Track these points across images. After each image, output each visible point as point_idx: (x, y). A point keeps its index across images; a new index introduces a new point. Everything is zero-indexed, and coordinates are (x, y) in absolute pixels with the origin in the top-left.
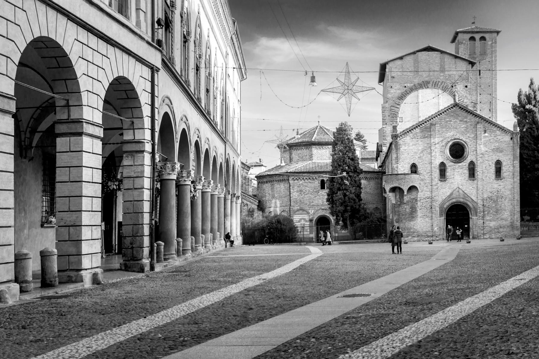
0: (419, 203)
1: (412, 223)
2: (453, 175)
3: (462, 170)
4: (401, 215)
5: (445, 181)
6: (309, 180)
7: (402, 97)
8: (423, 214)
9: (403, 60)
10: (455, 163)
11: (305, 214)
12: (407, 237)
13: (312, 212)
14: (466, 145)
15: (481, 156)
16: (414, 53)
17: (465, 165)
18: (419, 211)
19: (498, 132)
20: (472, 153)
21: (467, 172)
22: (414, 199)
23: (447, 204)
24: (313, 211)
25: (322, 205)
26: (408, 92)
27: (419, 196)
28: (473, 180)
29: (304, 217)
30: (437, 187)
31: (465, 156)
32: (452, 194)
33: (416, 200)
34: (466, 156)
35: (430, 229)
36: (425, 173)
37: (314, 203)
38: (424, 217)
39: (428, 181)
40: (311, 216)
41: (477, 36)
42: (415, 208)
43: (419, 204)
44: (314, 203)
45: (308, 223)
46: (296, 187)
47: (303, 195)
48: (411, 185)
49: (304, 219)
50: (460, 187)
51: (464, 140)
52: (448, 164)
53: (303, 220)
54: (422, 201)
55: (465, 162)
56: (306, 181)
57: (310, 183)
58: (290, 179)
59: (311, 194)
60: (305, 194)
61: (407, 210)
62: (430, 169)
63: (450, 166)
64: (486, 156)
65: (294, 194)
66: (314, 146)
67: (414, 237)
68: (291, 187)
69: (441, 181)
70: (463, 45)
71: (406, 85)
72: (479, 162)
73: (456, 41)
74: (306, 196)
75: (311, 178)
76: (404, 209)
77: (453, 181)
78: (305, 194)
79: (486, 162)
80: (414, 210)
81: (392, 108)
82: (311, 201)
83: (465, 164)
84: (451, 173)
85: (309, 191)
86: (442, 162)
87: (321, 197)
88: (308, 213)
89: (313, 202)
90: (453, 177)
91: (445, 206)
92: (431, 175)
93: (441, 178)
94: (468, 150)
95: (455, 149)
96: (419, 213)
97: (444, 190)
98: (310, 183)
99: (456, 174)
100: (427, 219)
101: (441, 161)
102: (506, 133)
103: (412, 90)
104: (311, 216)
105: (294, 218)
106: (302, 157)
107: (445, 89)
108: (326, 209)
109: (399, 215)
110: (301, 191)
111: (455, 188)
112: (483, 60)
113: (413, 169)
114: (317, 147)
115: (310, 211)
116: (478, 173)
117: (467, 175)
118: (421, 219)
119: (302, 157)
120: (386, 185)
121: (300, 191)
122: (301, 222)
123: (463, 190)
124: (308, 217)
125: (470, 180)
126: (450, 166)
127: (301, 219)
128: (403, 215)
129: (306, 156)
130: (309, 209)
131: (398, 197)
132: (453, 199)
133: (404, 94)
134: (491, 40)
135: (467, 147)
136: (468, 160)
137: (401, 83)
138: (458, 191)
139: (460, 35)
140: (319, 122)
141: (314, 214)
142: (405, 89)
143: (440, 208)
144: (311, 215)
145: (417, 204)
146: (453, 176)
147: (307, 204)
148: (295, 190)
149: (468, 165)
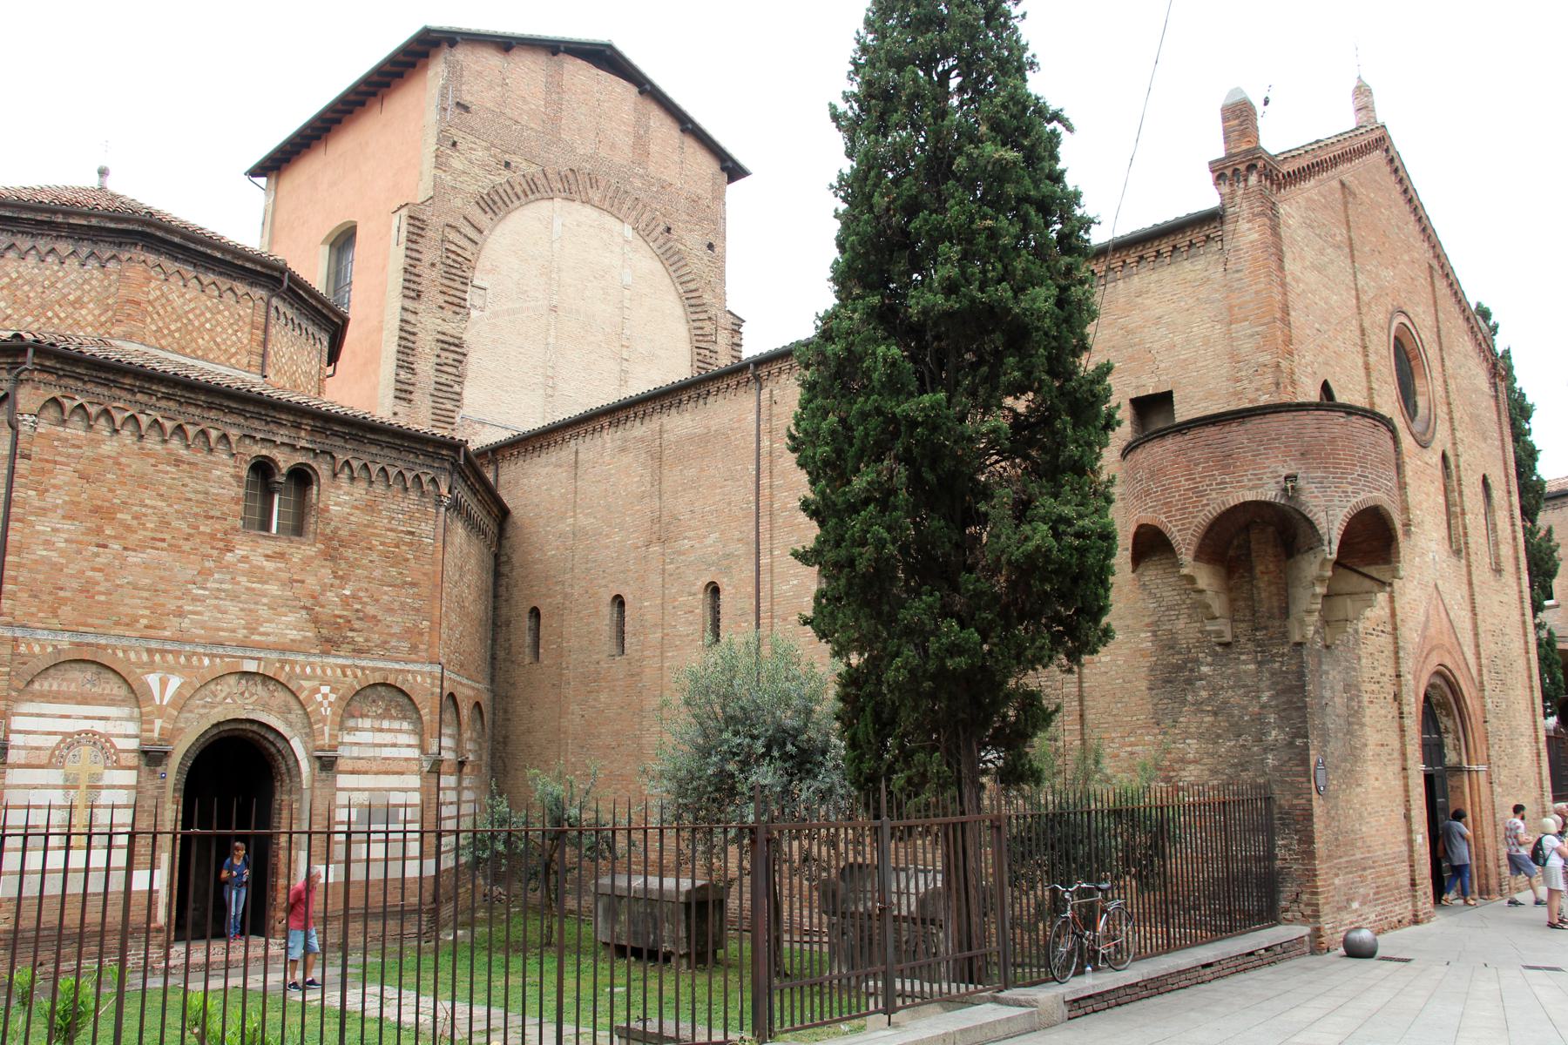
6: (175, 443)
7: (494, 204)
9: (509, 59)
11: (112, 702)
13: (165, 686)
16: (554, 48)
24: (175, 682)
25: (242, 645)
26: (518, 189)
29: (99, 726)
37: (186, 623)
40: (158, 723)
44: (186, 623)
45: (130, 777)
46: (63, 475)
47: (116, 546)
49: (100, 742)
53: (86, 751)
56: (152, 442)
57: (178, 462)
58: (28, 399)
59: (173, 547)
60: (133, 539)
65: (43, 527)
66: (152, 258)
68: (22, 466)
71: (515, 160)
74: (134, 558)
75: (191, 430)
78: (133, 539)
81: (453, 236)
82: (172, 605)
85: (164, 523)
87: (243, 580)
88: (136, 695)
89: (180, 614)
98: (178, 462)
103: (532, 190)
104: (158, 723)
105: (17, 723)
106: (43, 307)
107: (644, 233)
108: (266, 678)
110: (104, 513)
114: (170, 266)
115: (153, 680)
119: (43, 307)
121: (96, 510)
122: (71, 766)
124: (132, 728)
127: (71, 741)
129: (78, 303)
130: (151, 667)
133: (501, 191)
137: (493, 145)
140: (103, 172)
141: (182, 703)
142: (507, 174)
144: (161, 712)
148: (56, 498)
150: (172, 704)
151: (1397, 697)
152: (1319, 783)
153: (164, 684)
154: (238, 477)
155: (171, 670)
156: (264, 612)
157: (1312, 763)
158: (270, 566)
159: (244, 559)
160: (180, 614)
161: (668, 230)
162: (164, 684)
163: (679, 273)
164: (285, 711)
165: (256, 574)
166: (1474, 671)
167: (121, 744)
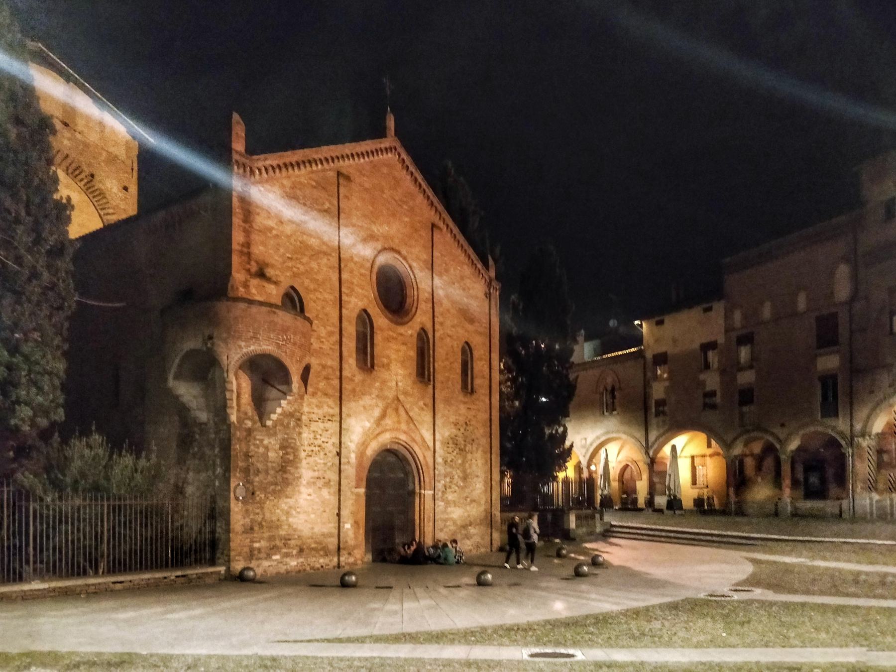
0: (306, 435)
1: (284, 503)
8: (316, 474)
12: (268, 557)
17: (411, 336)
18: (304, 462)
27: (306, 409)
33: (299, 420)
35: (331, 527)
38: (320, 483)
39: (329, 363)
42: (295, 450)
43: (304, 435)
54: (314, 426)
61: (271, 454)
67: (287, 555)
80: (291, 458)
83: (410, 331)
96: (306, 472)
100: (325, 493)
109: (246, 471)
118: (311, 491)
128: (258, 472)
145: (300, 433)
151: (339, 454)
152: (238, 495)
157: (232, 485)
166: (431, 444)
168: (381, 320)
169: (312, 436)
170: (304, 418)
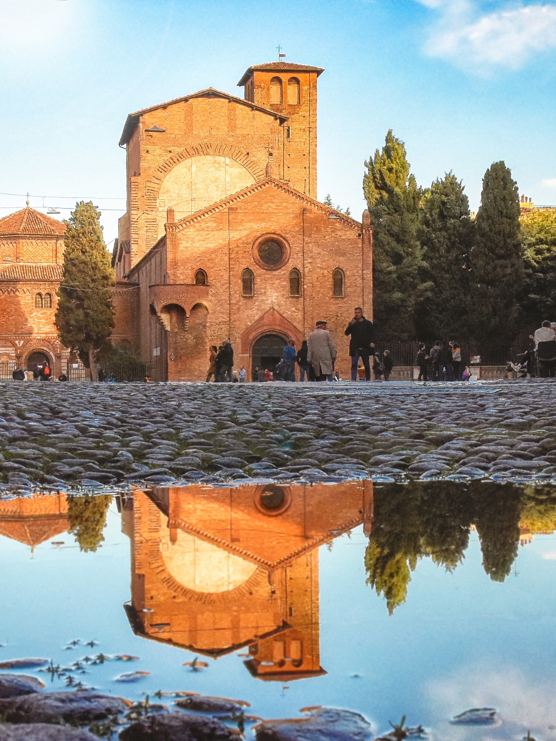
2: (265, 288)
3: (278, 281)
4: (179, 348)
5: (252, 297)
10: (267, 270)
14: (286, 243)
15: (310, 260)
17: (284, 274)
19: (337, 224)
20: (295, 256)
21: (286, 283)
22: (201, 324)
23: (254, 334)
24: (22, 342)
27: (208, 320)
28: (297, 298)
29: (7, 352)
30: (238, 306)
31: (284, 260)
32: (262, 318)
33: (205, 326)
34: (286, 260)
36: (219, 285)
39: (223, 298)
41: (285, 77)
42: (202, 338)
43: (208, 332)
48: (198, 302)
49: (8, 355)
50: (275, 308)
51: (283, 235)
52: (257, 271)
55: (283, 270)
62: (227, 278)
63: (260, 275)
64: (318, 261)
69: (244, 297)
70: (260, 89)
72: (307, 270)
73: (249, 83)
76: (185, 340)
77: (264, 298)
79: (318, 270)
80: (201, 342)
83: (284, 272)
84: (261, 285)
86: (248, 268)
87: (36, 320)
88: (14, 345)
89: (22, 328)
90: (265, 292)
91: (251, 337)
92: (229, 288)
93: (244, 293)
94: (289, 251)
95: (267, 248)
97: (249, 312)
99: (268, 288)
101: (244, 266)
102: (351, 226)
104: (19, 351)
111: (268, 308)
112: (293, 114)
113: (200, 277)
115: (17, 342)
116: (305, 286)
117: (288, 288)
120: (155, 302)
123: (281, 312)
125: (293, 297)
126: (260, 275)
128: (182, 349)
130: (16, 340)
131: (174, 319)
132: (264, 325)
134: (308, 83)
135: (287, 246)
136: (290, 265)
138: (273, 315)
139: (255, 73)
143: (242, 339)
144: (19, 348)
146: (263, 291)
147: (12, 330)
149: (288, 274)
150: (22, 346)
153: (19, 342)
154: (32, 298)
155: (21, 340)
156: (41, 326)
158: (42, 316)
159: (36, 315)
160: (22, 328)
161: (248, 154)
162: (19, 342)
163: (254, 169)
164: (48, 347)
165: (38, 318)
167: (12, 355)
168: (257, 271)
169: (212, 332)
170: (207, 324)
